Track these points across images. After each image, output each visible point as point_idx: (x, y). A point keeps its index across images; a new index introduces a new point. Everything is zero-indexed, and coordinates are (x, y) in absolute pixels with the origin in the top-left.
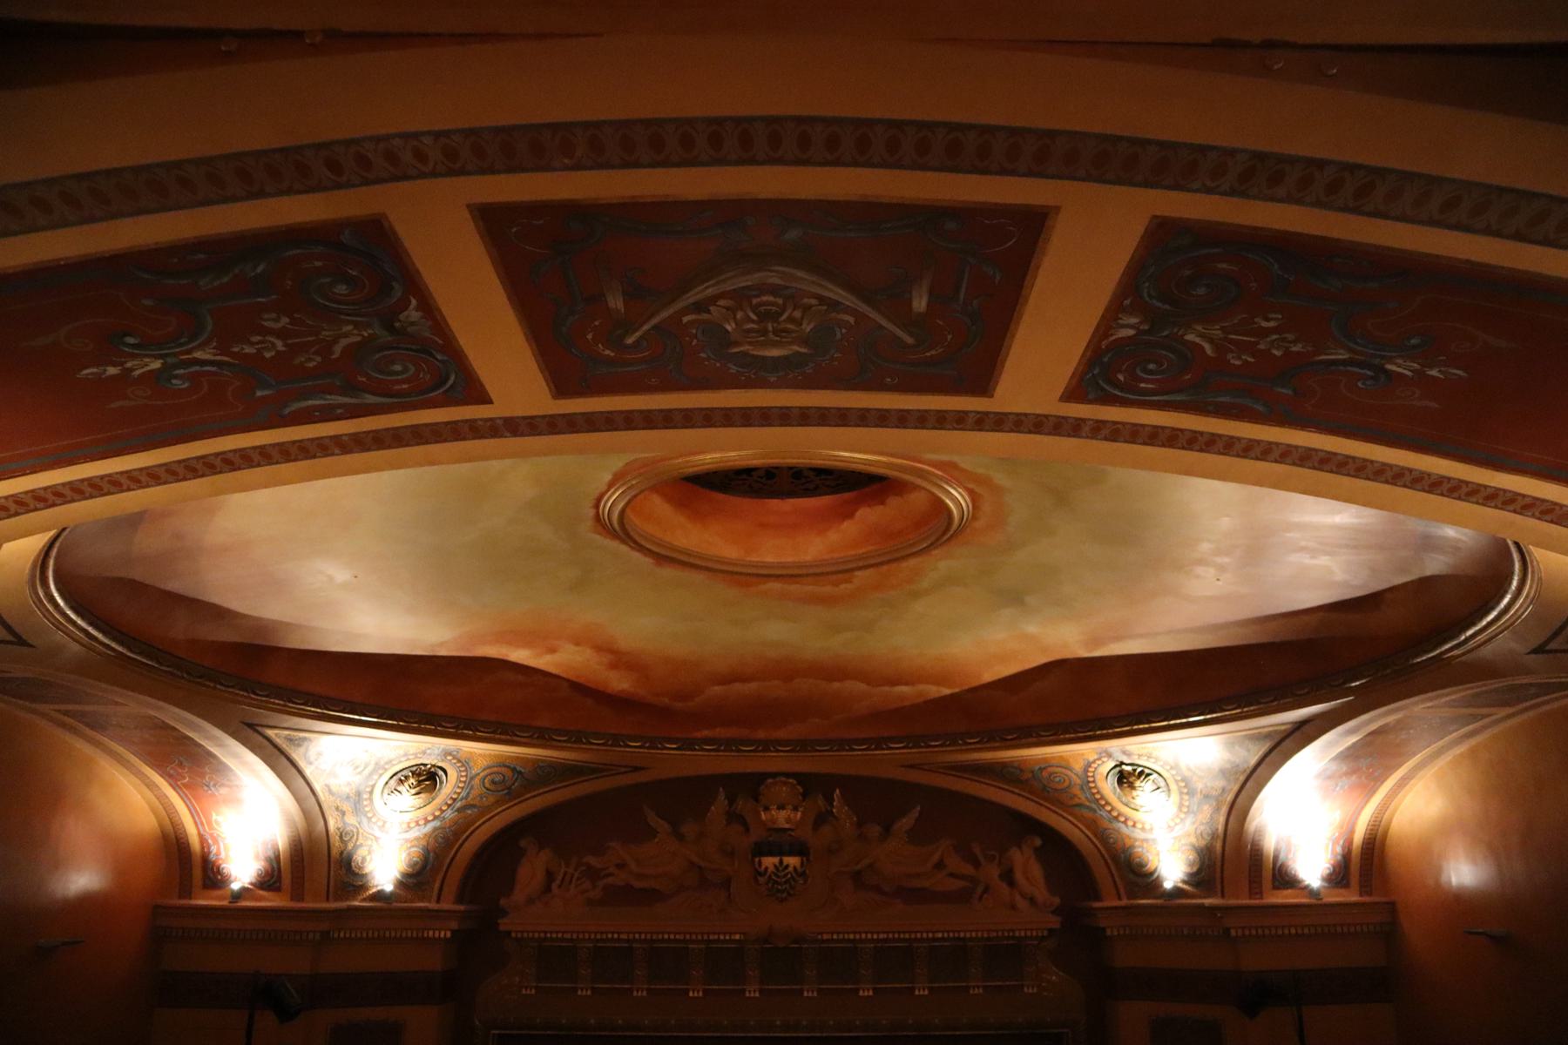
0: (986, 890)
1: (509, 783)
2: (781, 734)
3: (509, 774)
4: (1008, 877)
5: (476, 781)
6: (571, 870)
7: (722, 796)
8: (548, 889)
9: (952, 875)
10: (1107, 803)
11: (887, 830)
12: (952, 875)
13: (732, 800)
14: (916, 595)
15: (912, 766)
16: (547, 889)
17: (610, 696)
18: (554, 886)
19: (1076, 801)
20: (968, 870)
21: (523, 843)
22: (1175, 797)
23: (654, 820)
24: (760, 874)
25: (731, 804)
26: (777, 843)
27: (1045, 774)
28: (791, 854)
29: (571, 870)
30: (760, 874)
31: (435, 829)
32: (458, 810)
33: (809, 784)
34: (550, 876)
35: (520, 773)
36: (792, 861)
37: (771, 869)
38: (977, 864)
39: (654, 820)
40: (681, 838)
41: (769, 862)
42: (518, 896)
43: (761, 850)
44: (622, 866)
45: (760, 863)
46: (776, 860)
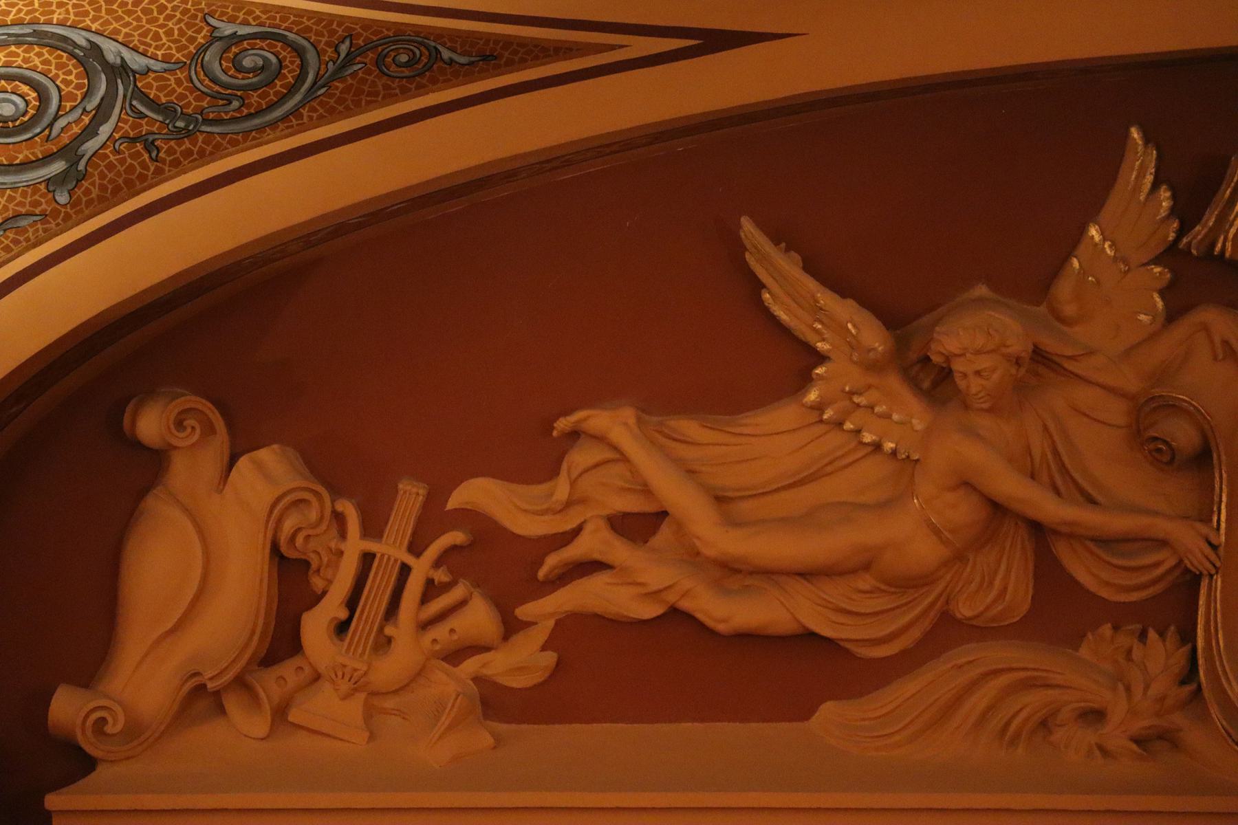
1: (69, 124)
6: (392, 549)
7: (1140, 160)
8: (282, 642)
13: (1194, 192)
16: (282, 642)
18: (315, 627)
21: (150, 424)
23: (793, 294)
25: (1187, 212)
29: (392, 549)
34: (291, 579)
35: (120, 71)
39: (793, 294)
40: (936, 382)
42: (142, 678)
44: (639, 526)
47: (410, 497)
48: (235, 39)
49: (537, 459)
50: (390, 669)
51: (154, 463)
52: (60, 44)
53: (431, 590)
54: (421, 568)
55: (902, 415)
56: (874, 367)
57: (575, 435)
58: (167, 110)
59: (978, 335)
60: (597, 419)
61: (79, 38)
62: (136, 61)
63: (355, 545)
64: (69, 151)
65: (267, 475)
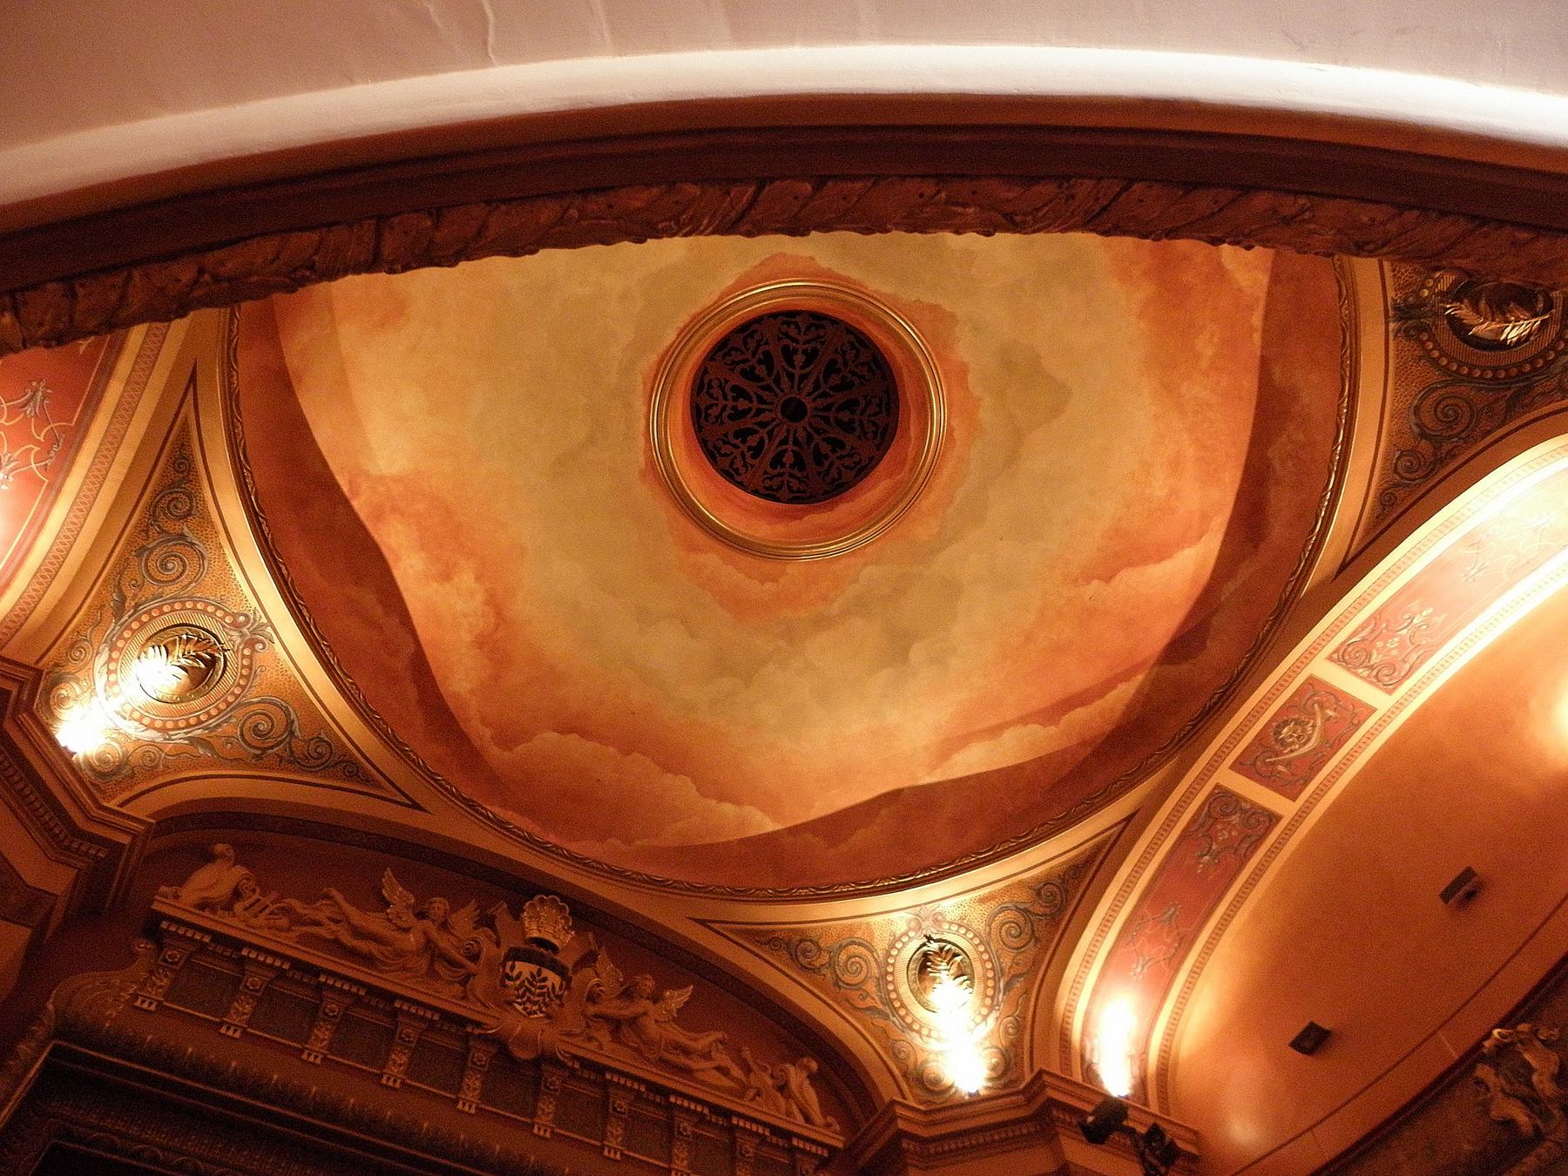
0: (758, 1094)
2: (574, 847)
3: (280, 726)
4: (783, 1088)
5: (240, 713)
6: (266, 900)
9: (718, 1069)
10: (903, 1006)
11: (656, 998)
12: (718, 1069)
14: (821, 623)
15: (702, 922)
17: (440, 697)
18: (238, 907)
19: (869, 1002)
20: (736, 1072)
22: (978, 986)
24: (510, 978)
26: (540, 953)
27: (843, 957)
28: (553, 969)
30: (510, 978)
31: (152, 743)
32: (194, 741)
33: (585, 913)
34: (237, 894)
35: (292, 733)
36: (553, 979)
37: (526, 974)
38: (748, 1070)
41: (524, 969)
43: (515, 955)
45: (512, 968)
46: (534, 968)
47: (274, 895)
48: (322, 740)
49: (309, 900)
50: (253, 921)
51: (210, 858)
52: (288, 715)
53: (272, 913)
54: (272, 908)
55: (409, 919)
56: (408, 907)
57: (328, 897)
58: (292, 752)
59: (439, 905)
60: (334, 892)
61: (293, 716)
62: (297, 733)
63: (257, 896)
64: (264, 750)
65: (240, 871)
